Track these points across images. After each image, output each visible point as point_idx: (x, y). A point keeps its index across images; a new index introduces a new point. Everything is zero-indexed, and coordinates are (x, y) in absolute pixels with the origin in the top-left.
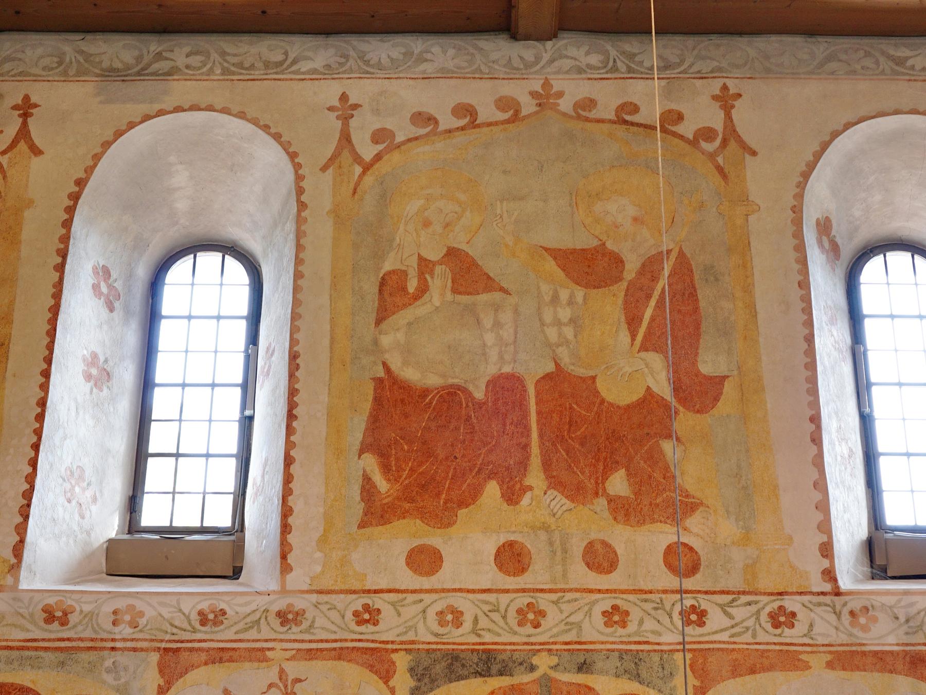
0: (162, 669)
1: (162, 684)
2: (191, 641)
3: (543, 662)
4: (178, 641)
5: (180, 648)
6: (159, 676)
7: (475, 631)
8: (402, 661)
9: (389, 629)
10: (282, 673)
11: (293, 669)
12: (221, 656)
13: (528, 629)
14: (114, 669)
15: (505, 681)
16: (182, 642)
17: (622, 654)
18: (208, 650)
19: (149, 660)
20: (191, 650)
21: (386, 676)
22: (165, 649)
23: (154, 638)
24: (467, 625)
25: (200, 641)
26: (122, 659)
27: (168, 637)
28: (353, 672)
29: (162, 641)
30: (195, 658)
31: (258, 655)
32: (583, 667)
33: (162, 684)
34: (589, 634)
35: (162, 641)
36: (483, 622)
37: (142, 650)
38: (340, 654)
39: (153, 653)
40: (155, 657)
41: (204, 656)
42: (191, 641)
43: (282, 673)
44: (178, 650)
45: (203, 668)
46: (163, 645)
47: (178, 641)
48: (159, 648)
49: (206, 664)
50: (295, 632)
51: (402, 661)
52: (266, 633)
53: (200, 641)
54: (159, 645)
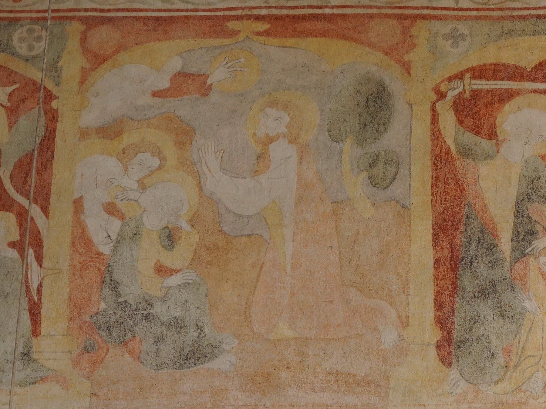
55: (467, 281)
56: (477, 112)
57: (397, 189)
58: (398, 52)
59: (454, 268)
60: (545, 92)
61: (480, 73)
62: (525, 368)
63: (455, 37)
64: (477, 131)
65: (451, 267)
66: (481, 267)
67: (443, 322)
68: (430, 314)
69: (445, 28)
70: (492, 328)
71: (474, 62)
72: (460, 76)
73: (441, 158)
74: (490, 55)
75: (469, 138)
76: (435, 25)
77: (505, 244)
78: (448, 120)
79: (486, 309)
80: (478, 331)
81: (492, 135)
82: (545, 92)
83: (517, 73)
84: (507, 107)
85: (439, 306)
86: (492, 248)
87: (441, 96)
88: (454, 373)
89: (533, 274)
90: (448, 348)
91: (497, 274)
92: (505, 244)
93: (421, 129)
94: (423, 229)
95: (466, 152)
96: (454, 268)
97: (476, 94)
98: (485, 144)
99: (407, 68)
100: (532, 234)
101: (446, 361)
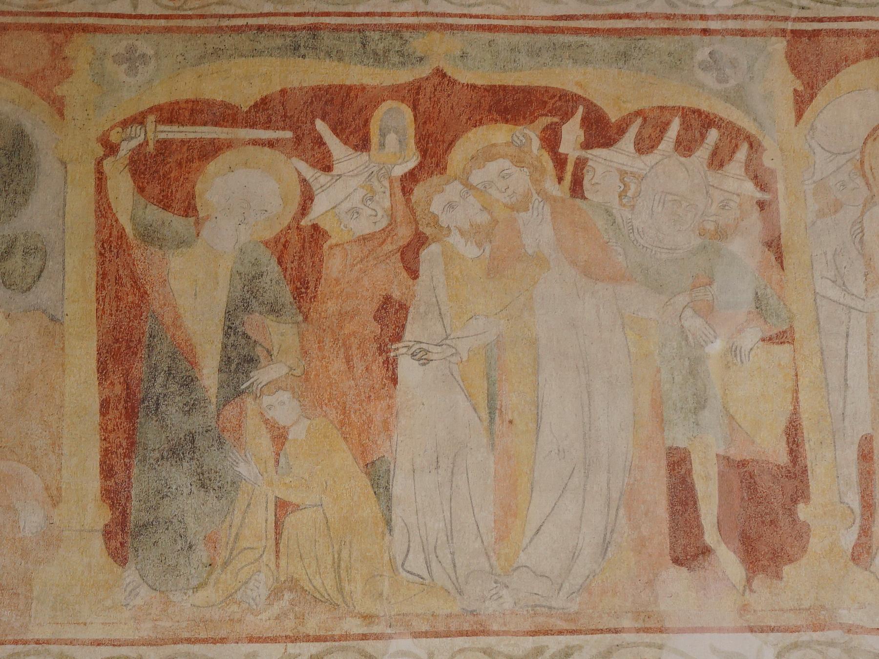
0: (795, 65)
1: (800, 88)
2: (836, 19)
4: (813, 20)
5: (820, 31)
6: (791, 76)
14: (714, 63)
16: (821, 20)
18: (867, 34)
19: (770, 49)
20: (839, 33)
22: (792, 31)
23: (772, 14)
25: (851, 19)
26: (728, 48)
27: (794, 13)
29: (786, 19)
30: (848, 46)
33: (800, 88)
35: (786, 19)
37: (755, 33)
39: (774, 39)
40: (779, 46)
41: (862, 45)
42: (836, 19)
44: (816, 33)
45: (864, 63)
46: (789, 26)
47: (813, 20)
48: (784, 31)
49: (868, 56)
53: (851, 19)
54: (782, 25)
55: (151, 434)
56: (167, 175)
57: (44, 293)
58: (44, 84)
59: (131, 414)
60: (3, 13)
61: (170, 114)
62: (239, 566)
63: (132, 60)
64: (166, 204)
65: (126, 411)
66: (173, 412)
67: (114, 496)
68: (94, 484)
69: (117, 45)
70: (189, 505)
71: (161, 97)
72: (139, 119)
73: (111, 245)
74: (186, 87)
75: (153, 214)
76: (102, 41)
77: (209, 377)
78: (122, 188)
79: (180, 476)
80: (168, 510)
81: (189, 209)
82: (3, 13)
83: (227, 115)
84: (212, 167)
85: (107, 472)
86: (189, 382)
87: (111, 149)
88: (130, 574)
89: (252, 423)
90: (122, 536)
91: (196, 422)
92: (209, 377)
93: (80, 201)
94: (83, 353)
95: (149, 236)
96: (131, 414)
97: (164, 146)
98: (178, 223)
99: (58, 106)
100: (250, 361)
101: (119, 555)
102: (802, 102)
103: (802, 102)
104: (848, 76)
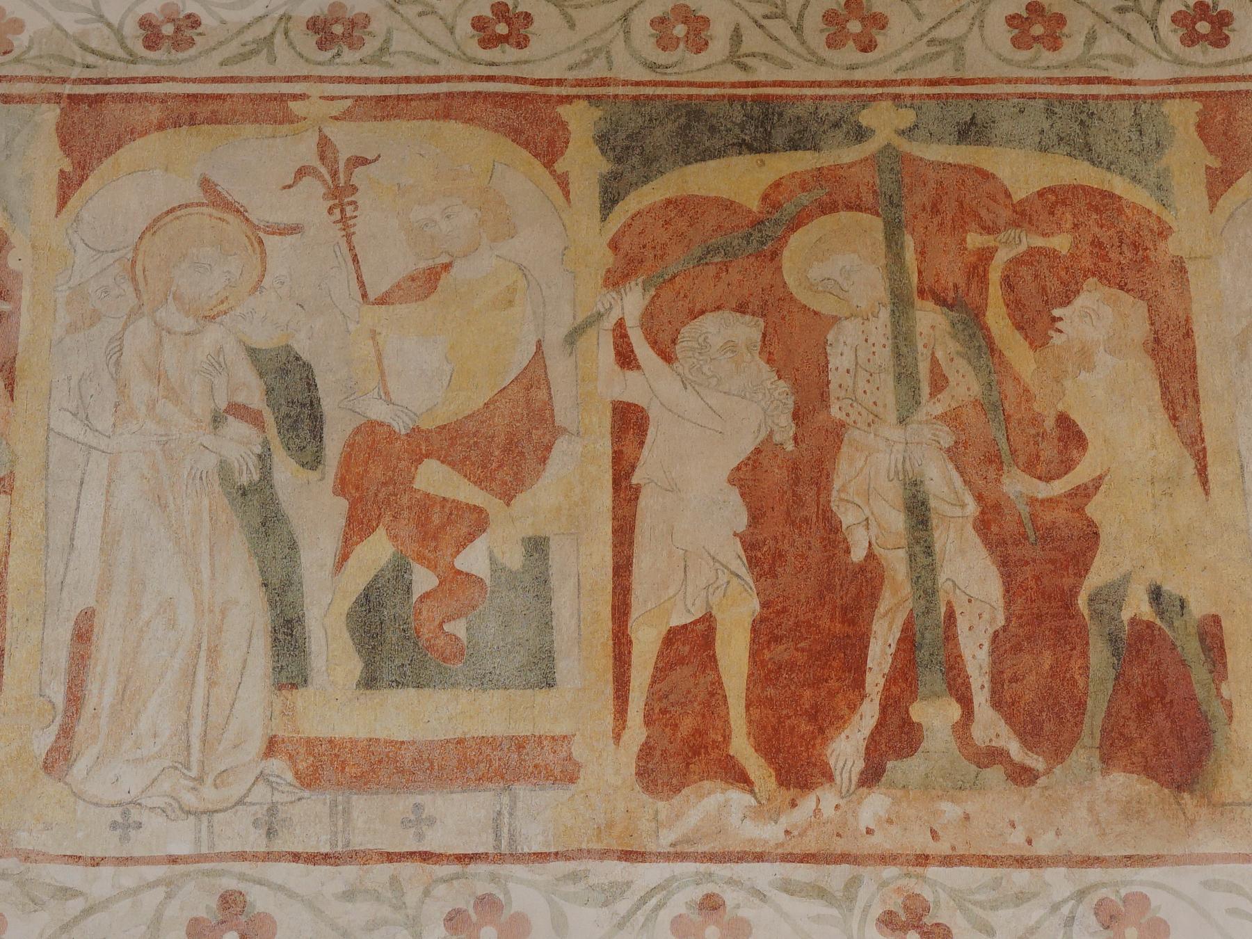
0: (66, 138)
1: (68, 169)
2: (126, 81)
3: (884, 123)
4: (98, 81)
5: (104, 95)
6: (59, 153)
7: (736, 58)
8: (580, 122)
9: (550, 53)
10: (325, 147)
11: (349, 139)
12: (194, 111)
13: (850, 54)
15: (804, 161)
16: (108, 82)
17: (1051, 104)
18: (164, 99)
19: (37, 118)
20: (128, 98)
21: (549, 151)
22: (69, 96)
23: (47, 74)
24: (719, 46)
25: (146, 80)
27: (76, 73)
28: (472, 144)
29: (64, 80)
30: (136, 115)
31: (271, 109)
32: (970, 132)
33: (68, 169)
34: (980, 62)
35: (64, 80)
36: (753, 40)
37: (21, 99)
38: (448, 107)
39: (45, 106)
40: (50, 115)
41: (155, 112)
42: (126, 81)
43: (325, 147)
44: (100, 98)
45: (154, 136)
46: (67, 89)
47: (98, 81)
48: (58, 96)
49: (161, 127)
50: (349, 61)
51: (580, 122)
52: (286, 64)
53: (146, 80)
54: (57, 89)
102: (67, 187)
103: (67, 187)
104: (129, 153)
